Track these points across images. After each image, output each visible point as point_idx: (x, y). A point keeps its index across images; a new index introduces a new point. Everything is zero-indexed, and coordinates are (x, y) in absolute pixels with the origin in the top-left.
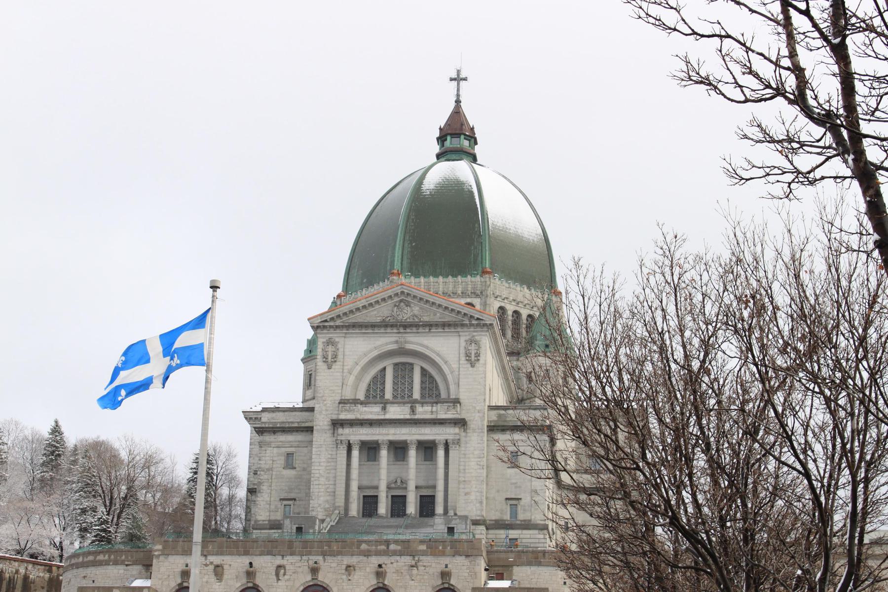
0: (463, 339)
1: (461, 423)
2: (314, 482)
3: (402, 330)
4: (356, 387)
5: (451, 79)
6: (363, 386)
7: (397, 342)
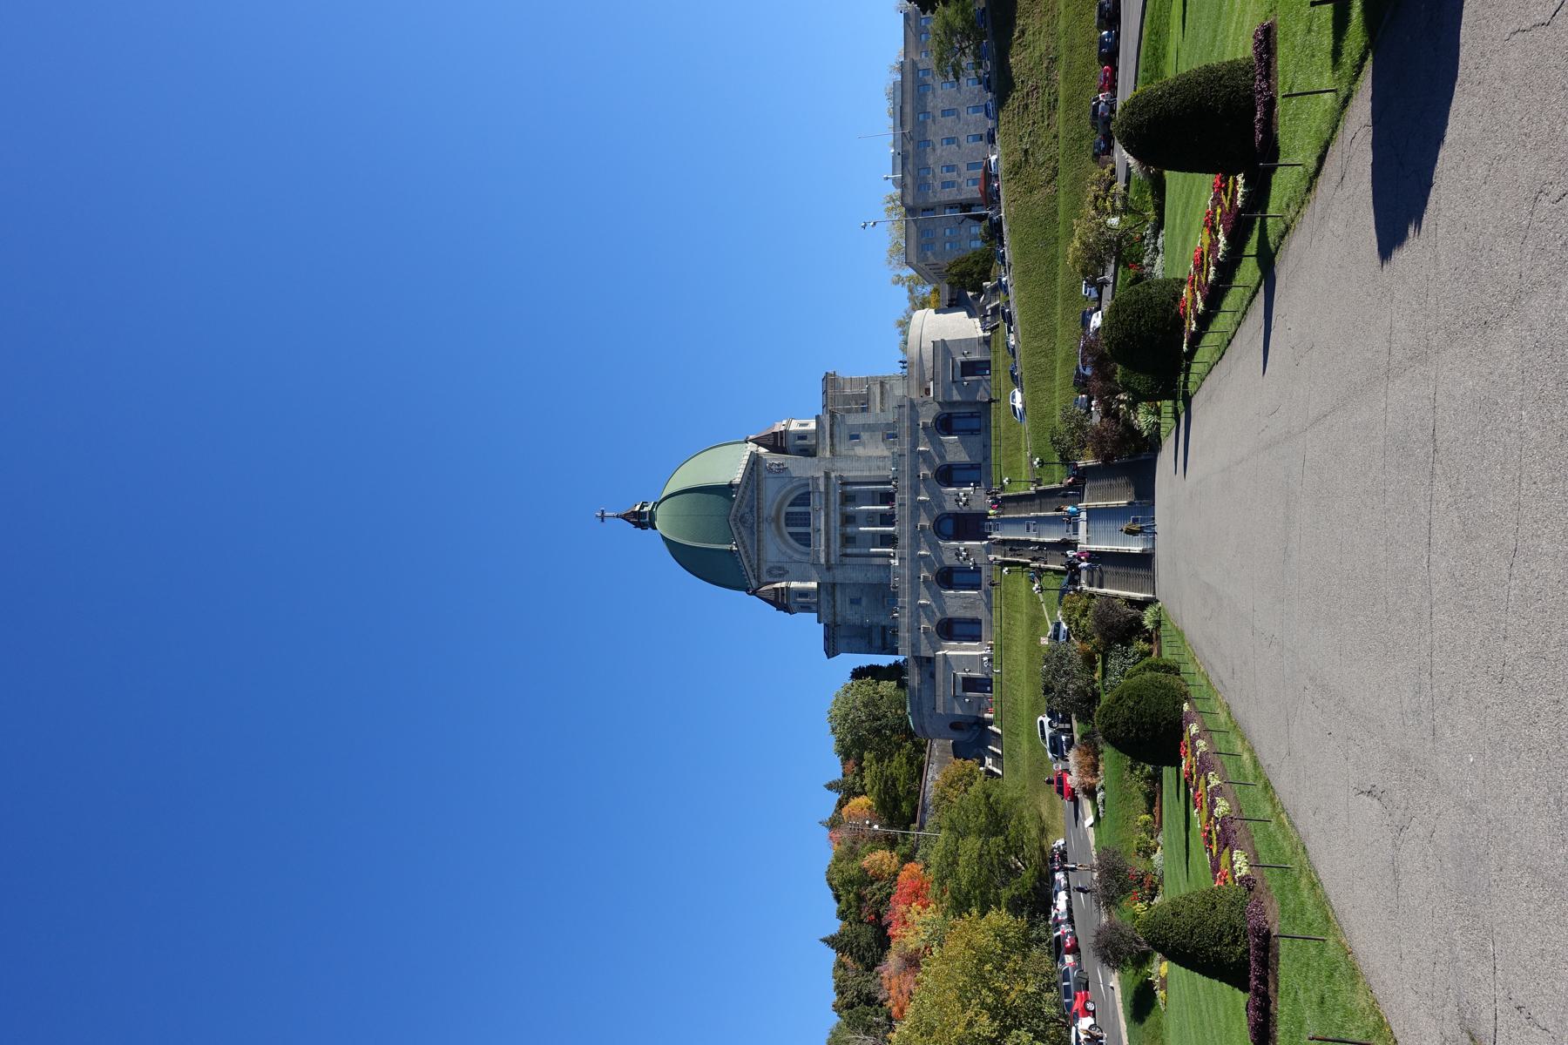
5: (603, 521)
6: (802, 548)
7: (770, 524)
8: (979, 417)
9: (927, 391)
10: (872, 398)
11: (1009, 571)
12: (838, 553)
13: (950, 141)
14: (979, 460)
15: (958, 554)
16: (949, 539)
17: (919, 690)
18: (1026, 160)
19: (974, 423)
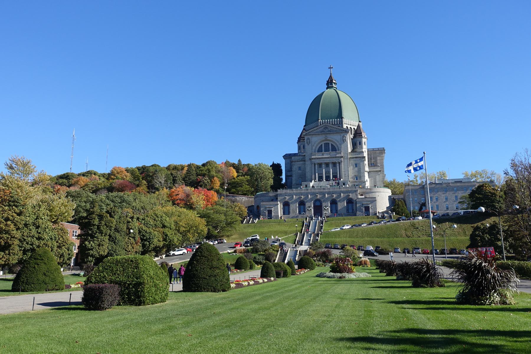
2: (306, 174)
6: (317, 149)
8: (353, 212)
9: (362, 195)
10: (375, 167)
11: (296, 227)
12: (315, 162)
13: (447, 199)
14: (339, 212)
15: (309, 207)
16: (314, 204)
17: (268, 196)
18: (415, 228)
19: (350, 211)
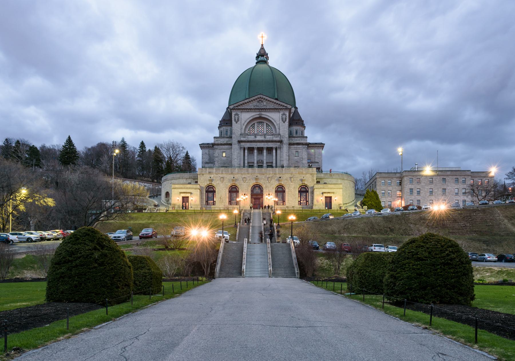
0: (281, 114)
1: (281, 142)
2: (233, 161)
3: (260, 110)
4: (245, 130)
7: (259, 114)
12: (245, 146)
